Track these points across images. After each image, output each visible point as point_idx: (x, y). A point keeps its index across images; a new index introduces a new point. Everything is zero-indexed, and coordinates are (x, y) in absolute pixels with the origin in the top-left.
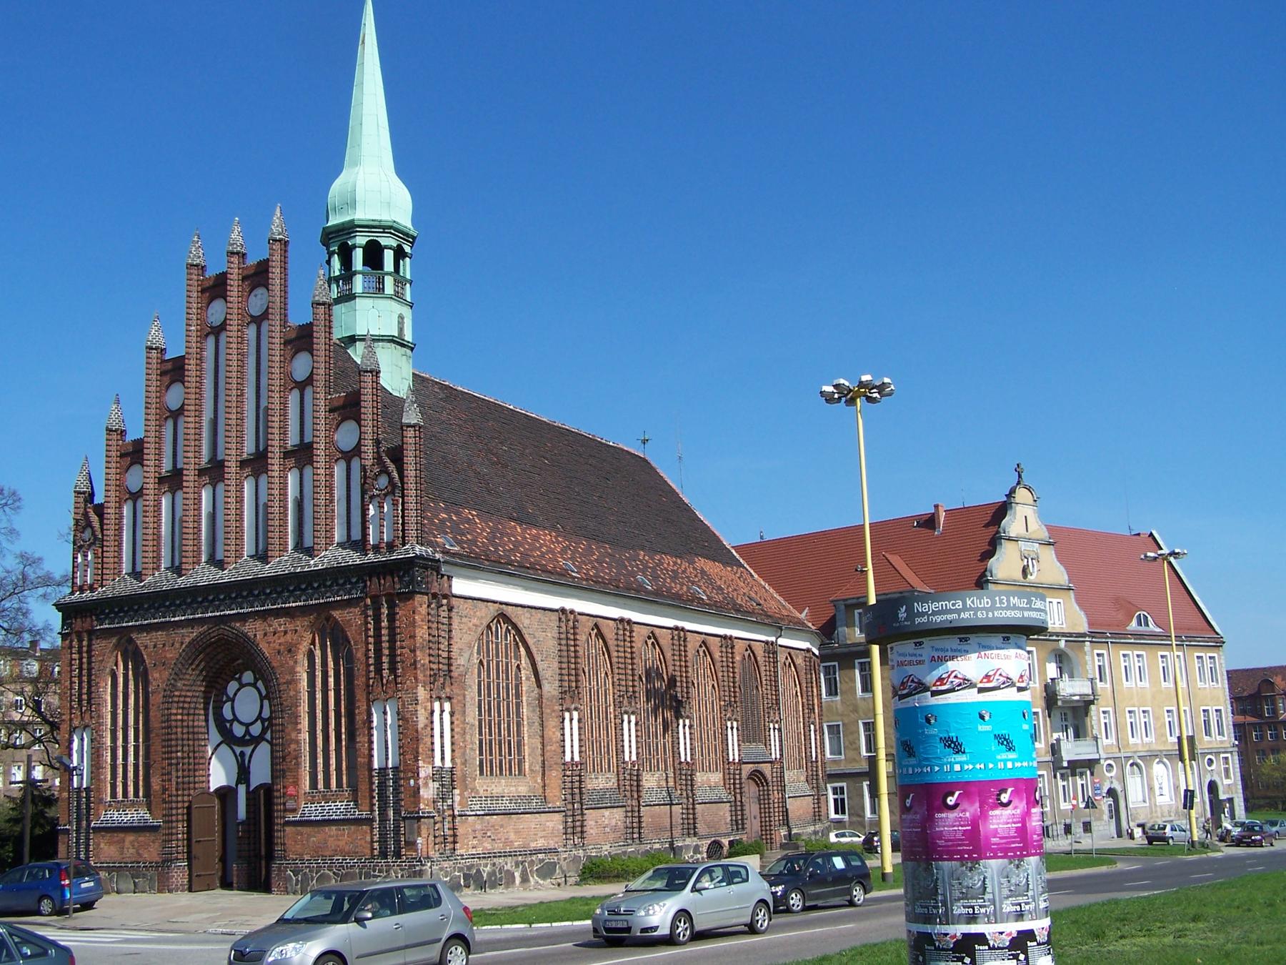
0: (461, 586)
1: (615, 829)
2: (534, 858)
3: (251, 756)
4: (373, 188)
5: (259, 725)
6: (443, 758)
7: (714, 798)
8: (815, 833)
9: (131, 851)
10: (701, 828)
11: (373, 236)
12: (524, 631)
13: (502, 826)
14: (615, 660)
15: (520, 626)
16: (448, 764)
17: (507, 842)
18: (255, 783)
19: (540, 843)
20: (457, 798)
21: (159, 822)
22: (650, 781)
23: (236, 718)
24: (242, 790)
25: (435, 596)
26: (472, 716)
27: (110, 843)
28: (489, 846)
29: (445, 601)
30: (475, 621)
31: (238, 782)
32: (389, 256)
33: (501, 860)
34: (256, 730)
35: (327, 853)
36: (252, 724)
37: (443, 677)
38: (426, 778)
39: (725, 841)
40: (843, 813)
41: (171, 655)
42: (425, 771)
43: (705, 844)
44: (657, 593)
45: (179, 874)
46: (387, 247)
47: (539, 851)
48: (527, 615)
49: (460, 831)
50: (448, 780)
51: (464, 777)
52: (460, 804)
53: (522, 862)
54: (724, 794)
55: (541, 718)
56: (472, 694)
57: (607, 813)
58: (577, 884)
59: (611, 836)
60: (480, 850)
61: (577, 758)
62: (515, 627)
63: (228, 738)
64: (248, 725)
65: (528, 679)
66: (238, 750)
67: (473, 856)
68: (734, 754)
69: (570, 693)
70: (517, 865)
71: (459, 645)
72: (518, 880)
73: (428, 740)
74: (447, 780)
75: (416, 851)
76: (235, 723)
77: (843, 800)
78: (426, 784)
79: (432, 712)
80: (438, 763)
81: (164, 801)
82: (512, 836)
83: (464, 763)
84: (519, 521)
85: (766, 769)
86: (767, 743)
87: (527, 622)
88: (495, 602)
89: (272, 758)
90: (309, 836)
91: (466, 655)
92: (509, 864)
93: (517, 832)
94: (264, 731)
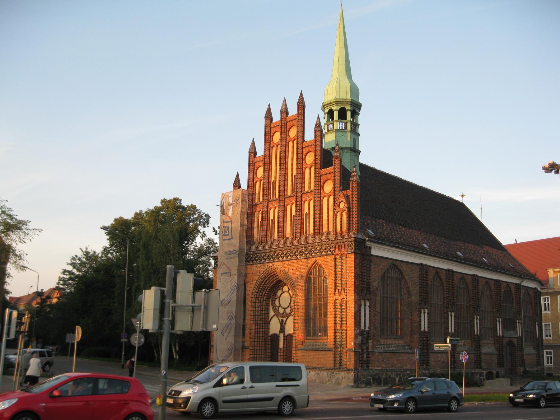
3: (286, 321)
5: (289, 309)
8: (537, 371)
10: (483, 365)
11: (343, 106)
13: (391, 358)
14: (445, 288)
16: (367, 329)
18: (287, 333)
20: (370, 344)
23: (280, 306)
24: (281, 336)
25: (363, 255)
28: (385, 366)
29: (368, 258)
30: (381, 267)
32: (349, 114)
33: (390, 373)
34: (288, 311)
39: (494, 372)
40: (551, 363)
43: (485, 372)
46: (348, 110)
47: (408, 370)
48: (405, 265)
49: (372, 358)
52: (372, 346)
53: (400, 375)
54: (495, 352)
56: (378, 299)
57: (440, 355)
60: (380, 368)
61: (426, 330)
62: (400, 270)
63: (277, 314)
64: (285, 309)
68: (500, 332)
69: (424, 301)
77: (551, 357)
80: (362, 328)
82: (395, 363)
83: (375, 329)
85: (515, 341)
87: (405, 269)
94: (292, 311)
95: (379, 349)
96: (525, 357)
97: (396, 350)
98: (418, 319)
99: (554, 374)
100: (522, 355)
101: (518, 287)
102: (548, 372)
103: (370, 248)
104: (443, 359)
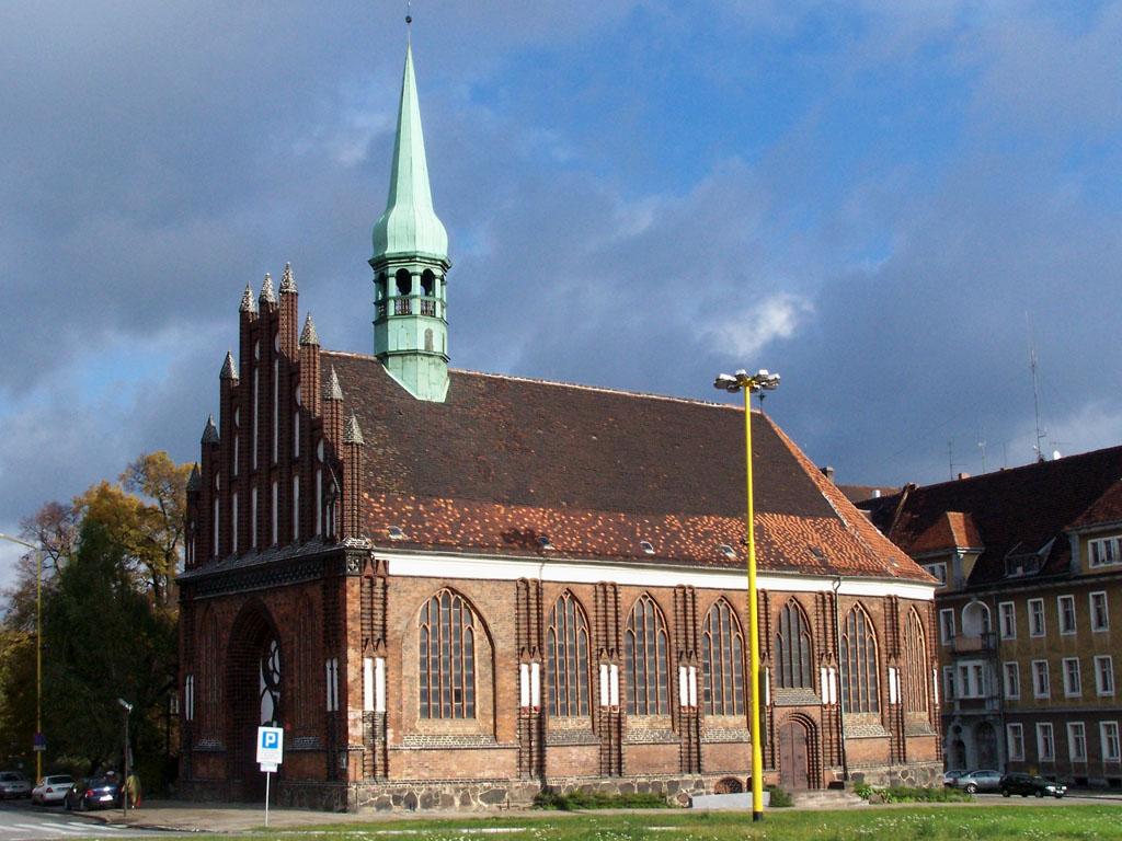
0: (399, 564)
1: (585, 764)
2: (478, 786)
6: (333, 705)
7: (731, 738)
8: (890, 773)
10: (707, 764)
12: (473, 600)
13: (441, 759)
15: (469, 596)
17: (447, 771)
19: (488, 774)
22: (637, 725)
26: (412, 669)
28: (426, 775)
33: (439, 787)
37: (378, 640)
38: (355, 720)
42: (353, 714)
44: (652, 558)
47: (487, 780)
48: (477, 586)
50: (379, 725)
51: (399, 720)
52: (394, 740)
55: (494, 670)
57: (574, 750)
58: (531, 808)
59: (581, 770)
60: (415, 777)
63: (271, 686)
65: (480, 638)
67: (406, 782)
70: (457, 790)
71: (397, 614)
72: (457, 802)
73: (359, 691)
74: (379, 722)
78: (355, 725)
79: (362, 669)
82: (454, 767)
84: (507, 504)
86: (814, 684)
88: (439, 578)
89: (620, 689)
91: (404, 623)
92: (448, 790)
93: (460, 764)
95: (413, 742)
96: (848, 746)
97: (456, 743)
98: (514, 684)
99: (1089, 780)
100: (840, 743)
101: (828, 601)
102: (1078, 775)
103: (385, 563)
104: (584, 758)
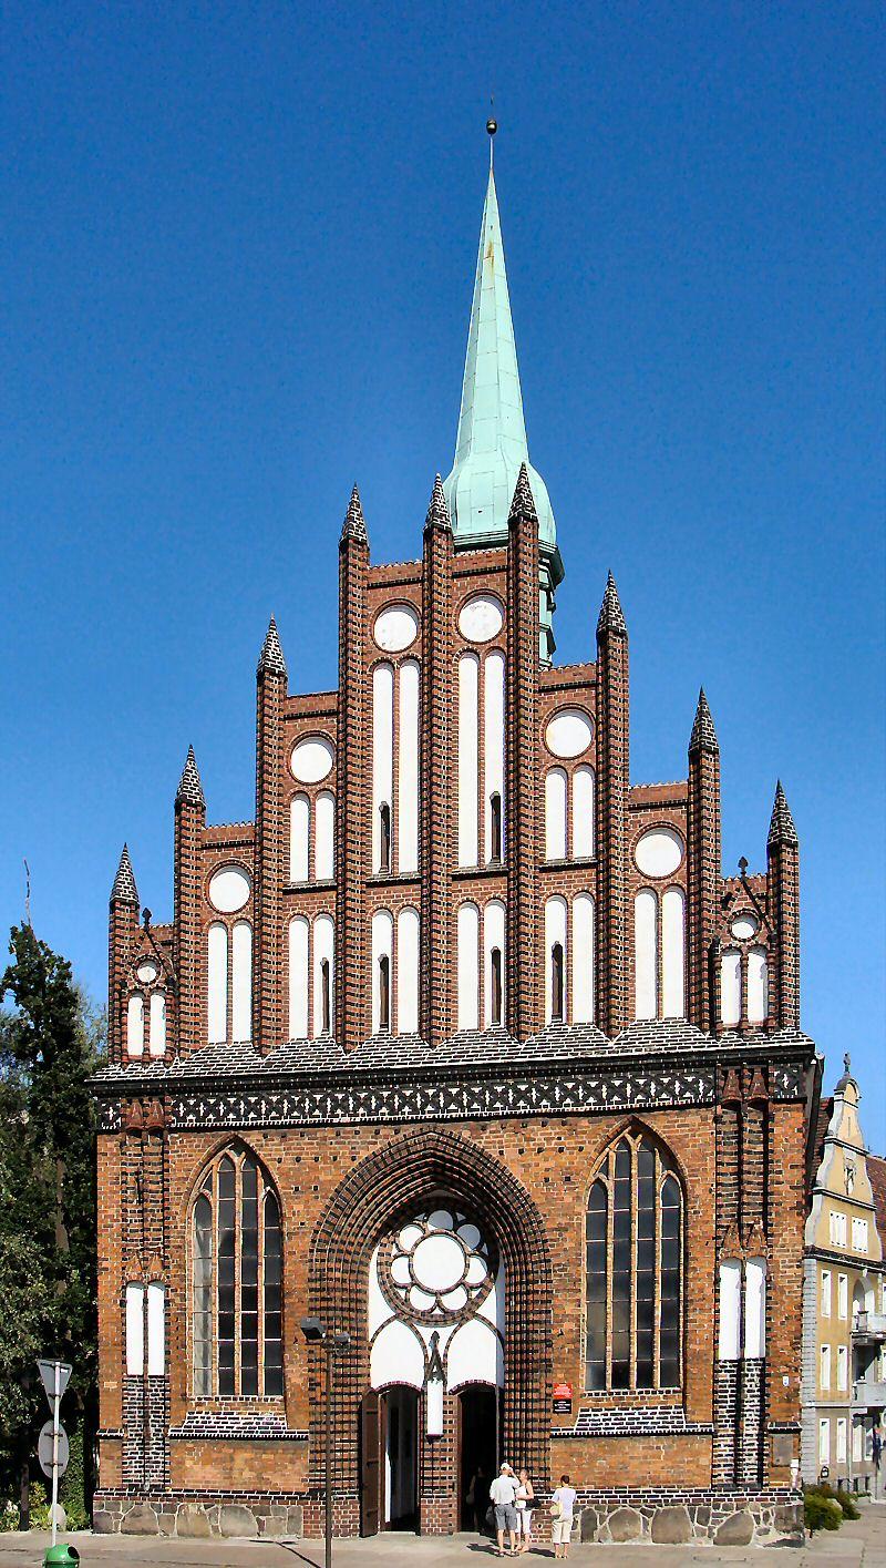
4: (490, 467)
9: (247, 1474)
18: (456, 1378)
21: (302, 1426)
27: (206, 1461)
31: (429, 1376)
34: (456, 1301)
35: (627, 1483)
36: (449, 1291)
41: (330, 1176)
45: (347, 1512)
63: (404, 1313)
66: (427, 1332)
75: (788, 1479)
76: (414, 1289)
81: (313, 1402)
90: (593, 1458)
